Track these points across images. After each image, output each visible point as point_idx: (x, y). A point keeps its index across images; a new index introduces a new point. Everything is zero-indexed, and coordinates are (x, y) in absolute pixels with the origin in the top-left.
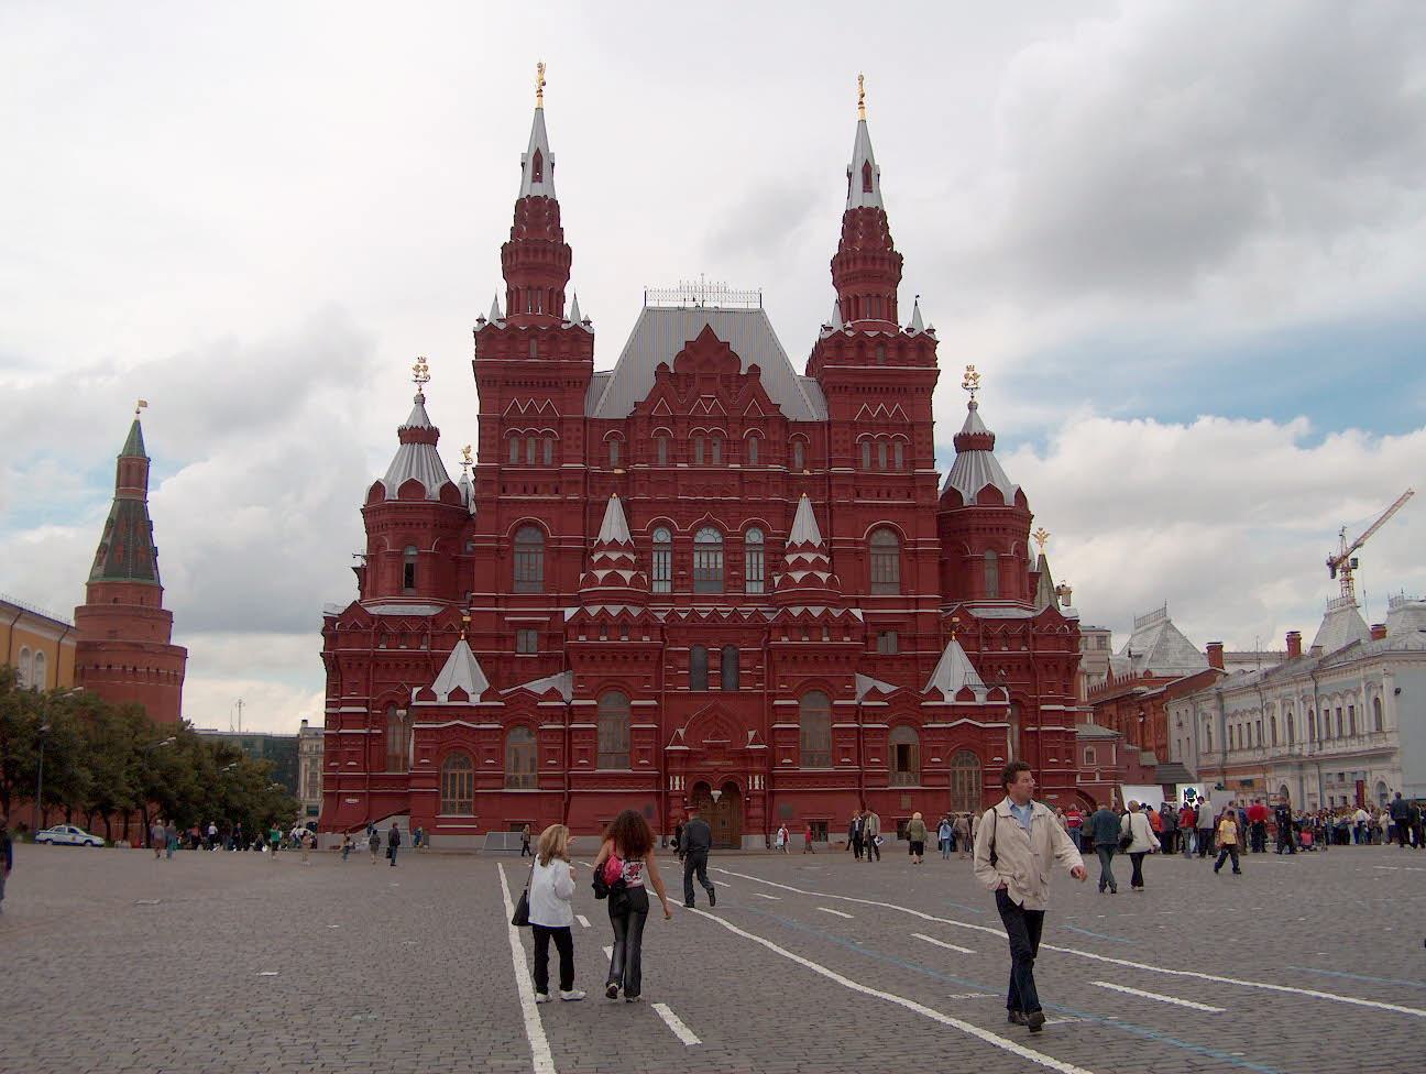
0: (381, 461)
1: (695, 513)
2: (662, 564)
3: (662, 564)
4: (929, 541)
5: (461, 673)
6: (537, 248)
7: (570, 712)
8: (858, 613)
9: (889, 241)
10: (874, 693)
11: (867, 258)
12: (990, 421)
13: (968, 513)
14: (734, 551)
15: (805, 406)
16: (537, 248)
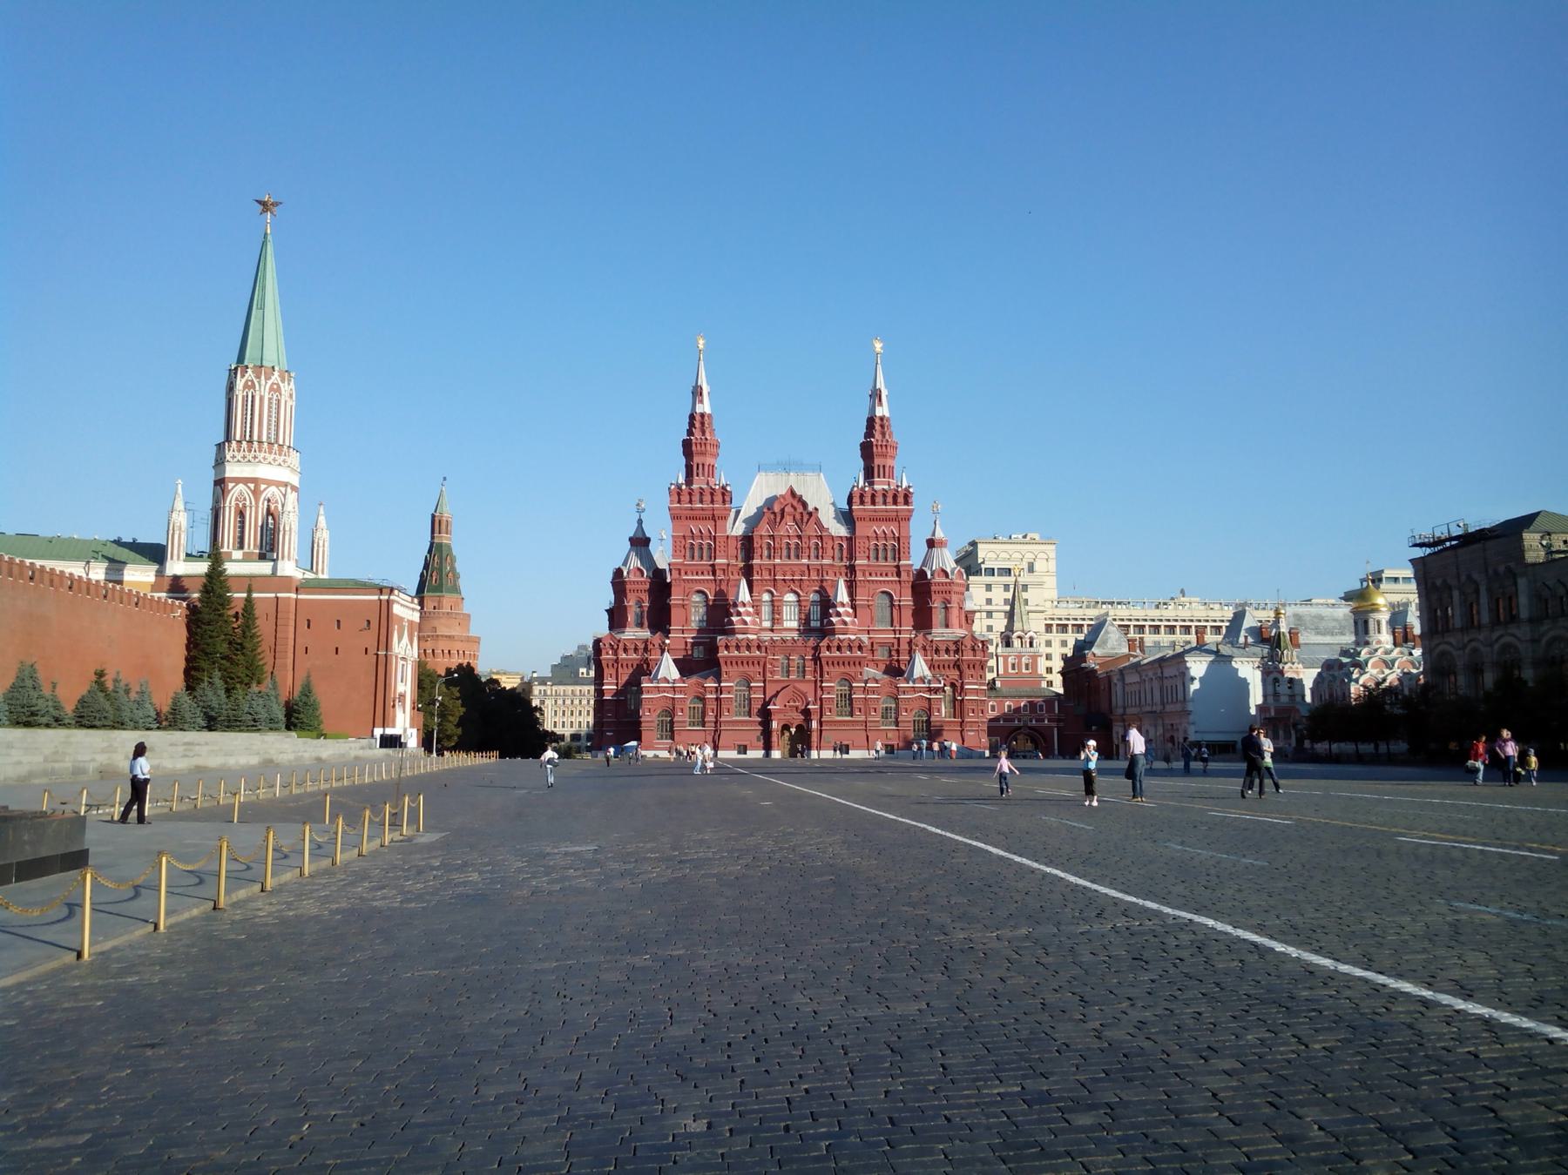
2: (766, 610)
8: (865, 638)
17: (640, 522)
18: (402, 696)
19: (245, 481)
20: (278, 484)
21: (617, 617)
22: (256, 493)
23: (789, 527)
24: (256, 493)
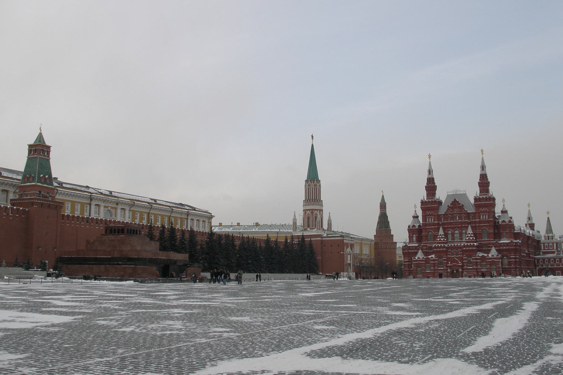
0: (409, 221)
1: (453, 228)
3: (450, 236)
4: (492, 231)
5: (420, 255)
6: (431, 187)
7: (434, 260)
8: (475, 244)
9: (487, 179)
10: (479, 256)
11: (484, 183)
12: (507, 208)
13: (500, 225)
14: (461, 234)
15: (471, 210)
16: (431, 187)
17: (415, 211)
18: (349, 264)
19: (309, 210)
20: (317, 210)
21: (411, 238)
22: (312, 213)
23: (456, 211)
24: (312, 213)
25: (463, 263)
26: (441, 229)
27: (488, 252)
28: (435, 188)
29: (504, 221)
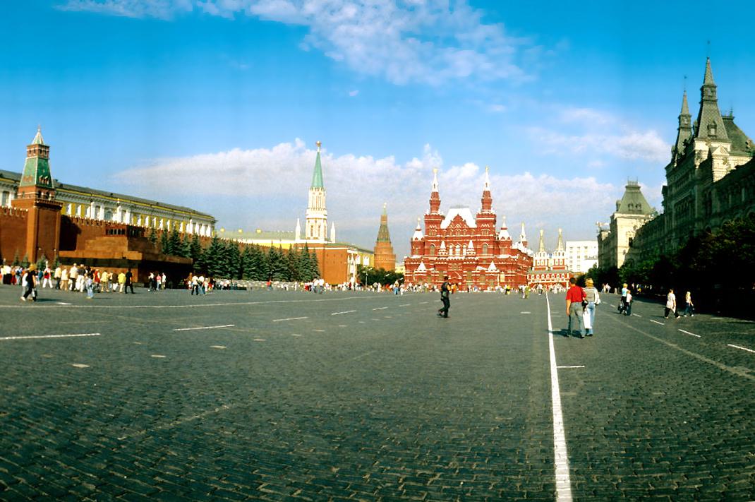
2: (451, 251)
3: (451, 251)
5: (422, 267)
7: (435, 273)
14: (462, 249)
18: (352, 274)
23: (458, 226)
25: (463, 277)
26: (443, 243)
27: (488, 266)
28: (438, 203)
29: (503, 238)
